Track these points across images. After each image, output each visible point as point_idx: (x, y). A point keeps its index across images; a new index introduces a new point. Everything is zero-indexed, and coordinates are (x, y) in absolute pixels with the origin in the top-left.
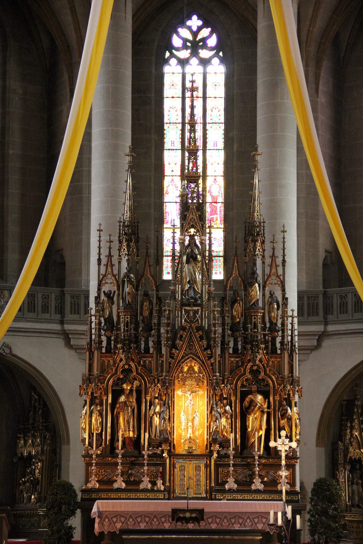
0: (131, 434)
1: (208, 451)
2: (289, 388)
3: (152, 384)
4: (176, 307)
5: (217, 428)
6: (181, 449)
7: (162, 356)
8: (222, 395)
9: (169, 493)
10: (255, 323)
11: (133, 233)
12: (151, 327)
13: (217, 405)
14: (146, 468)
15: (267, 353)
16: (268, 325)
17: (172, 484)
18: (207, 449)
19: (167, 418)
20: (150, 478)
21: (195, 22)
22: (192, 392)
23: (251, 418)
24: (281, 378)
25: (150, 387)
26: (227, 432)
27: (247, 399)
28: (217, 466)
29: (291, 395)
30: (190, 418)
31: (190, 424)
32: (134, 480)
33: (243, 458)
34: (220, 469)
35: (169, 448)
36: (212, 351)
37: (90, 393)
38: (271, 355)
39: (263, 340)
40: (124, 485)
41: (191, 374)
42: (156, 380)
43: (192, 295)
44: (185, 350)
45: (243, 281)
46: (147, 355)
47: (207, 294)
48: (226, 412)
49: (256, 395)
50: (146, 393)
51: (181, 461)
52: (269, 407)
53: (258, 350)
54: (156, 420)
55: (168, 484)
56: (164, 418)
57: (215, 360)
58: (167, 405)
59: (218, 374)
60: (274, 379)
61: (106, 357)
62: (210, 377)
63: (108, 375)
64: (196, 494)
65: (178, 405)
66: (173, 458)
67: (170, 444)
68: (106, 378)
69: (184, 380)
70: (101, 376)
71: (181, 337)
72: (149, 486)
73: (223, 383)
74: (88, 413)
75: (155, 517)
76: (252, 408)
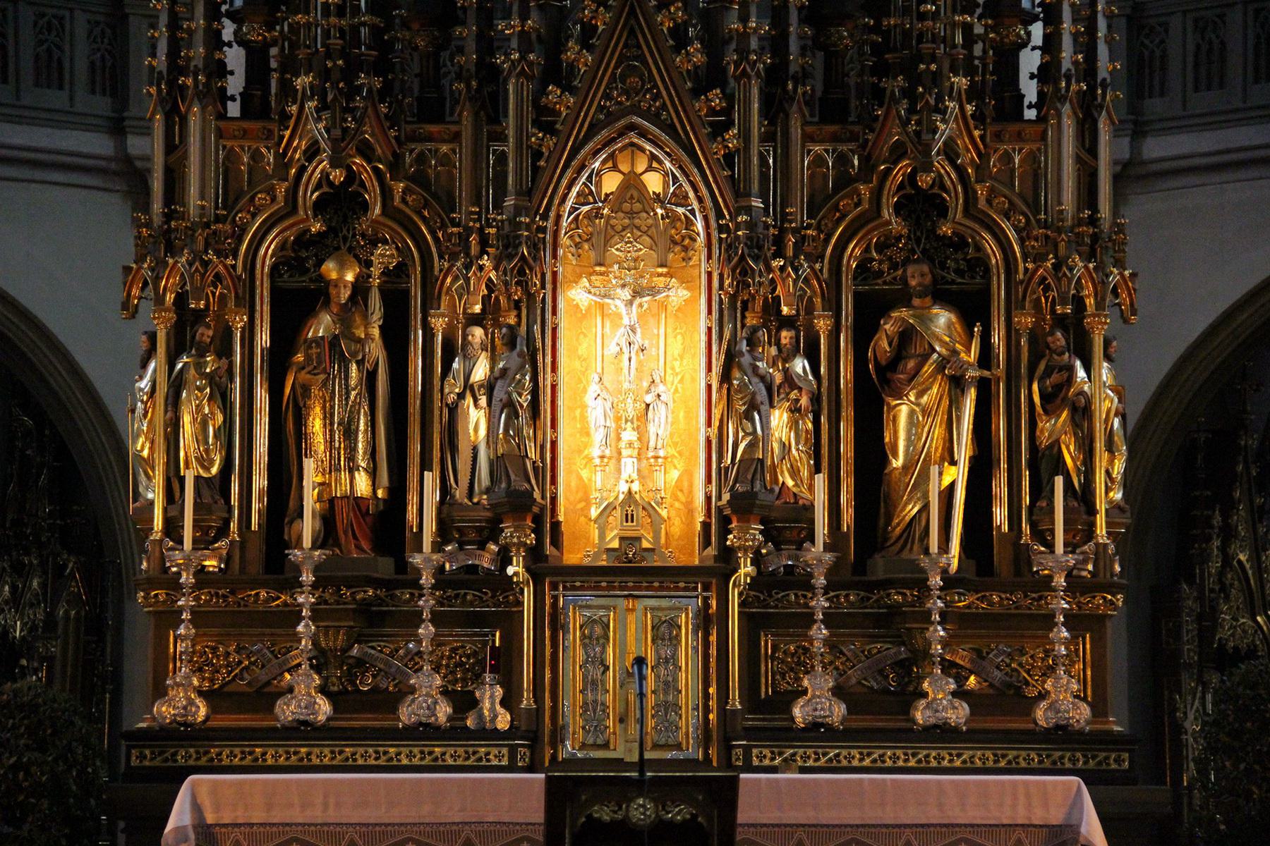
0: (362, 484)
1: (711, 551)
3: (454, 257)
5: (752, 446)
8: (772, 307)
14: (426, 630)
15: (979, 117)
17: (548, 702)
18: (706, 542)
19: (525, 400)
20: (449, 676)
22: (637, 293)
26: (794, 473)
28: (753, 624)
30: (631, 409)
31: (629, 435)
32: (375, 690)
33: (870, 587)
35: (531, 539)
37: (170, 298)
38: (997, 127)
40: (324, 708)
42: (474, 239)
44: (607, 96)
48: (789, 380)
50: (430, 301)
51: (588, 598)
52: (986, 358)
53: (939, 98)
54: (475, 419)
55: (527, 701)
60: (1012, 235)
61: (245, 134)
62: (720, 215)
63: (254, 216)
66: (554, 587)
67: (538, 520)
68: (244, 231)
70: (218, 219)
72: (444, 711)
74: (162, 389)
76: (911, 364)
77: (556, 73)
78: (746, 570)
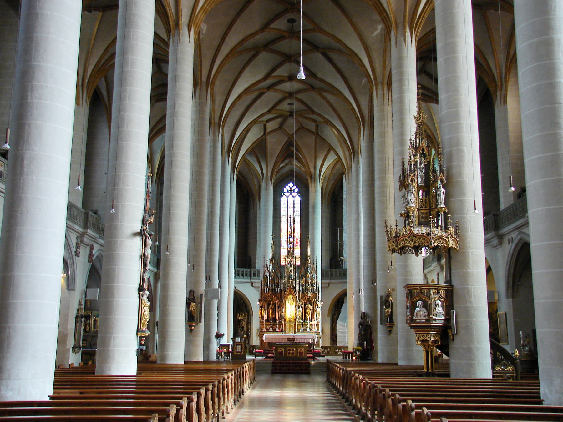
11: (273, 258)
21: (291, 184)
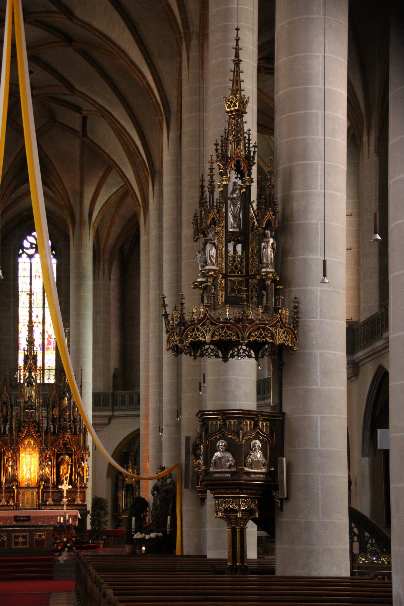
1: (38, 485)
2: (83, 452)
3: (7, 451)
4: (21, 410)
6: (24, 484)
7: (13, 435)
8: (46, 456)
9: (17, 507)
10: (65, 418)
12: (7, 420)
13: (43, 462)
14: (4, 494)
16: (72, 419)
22: (30, 455)
23: (62, 467)
24: (79, 447)
25: (6, 452)
26: (48, 475)
27: (60, 458)
29: (84, 455)
30: (29, 468)
31: (28, 471)
34: (45, 494)
36: (40, 434)
39: (69, 427)
41: (29, 445)
43: (30, 403)
45: (59, 396)
46: (5, 435)
47: (38, 404)
48: (48, 464)
49: (65, 456)
52: (72, 462)
54: (10, 469)
55: (16, 502)
56: (14, 469)
57: (42, 438)
58: (15, 462)
59: (44, 446)
60: (75, 447)
64: (31, 507)
65: (22, 461)
69: (25, 448)
71: (24, 426)
72: (6, 503)
73: (47, 450)
75: (8, 519)
77: (20, 431)
78: (42, 487)
